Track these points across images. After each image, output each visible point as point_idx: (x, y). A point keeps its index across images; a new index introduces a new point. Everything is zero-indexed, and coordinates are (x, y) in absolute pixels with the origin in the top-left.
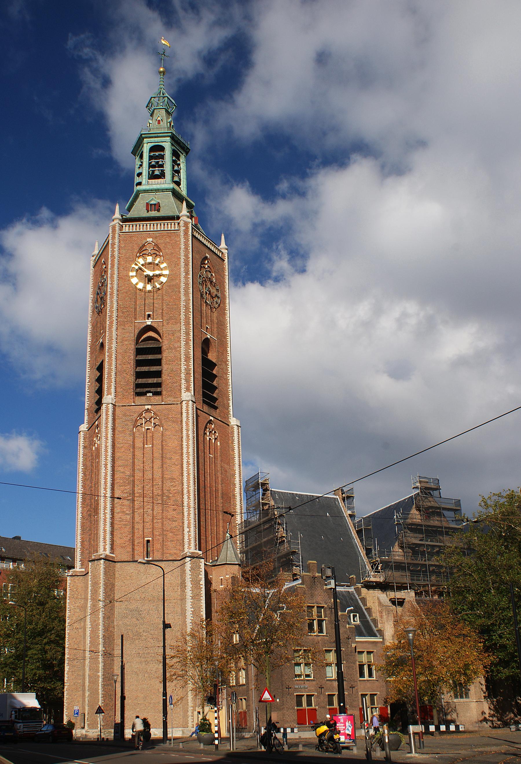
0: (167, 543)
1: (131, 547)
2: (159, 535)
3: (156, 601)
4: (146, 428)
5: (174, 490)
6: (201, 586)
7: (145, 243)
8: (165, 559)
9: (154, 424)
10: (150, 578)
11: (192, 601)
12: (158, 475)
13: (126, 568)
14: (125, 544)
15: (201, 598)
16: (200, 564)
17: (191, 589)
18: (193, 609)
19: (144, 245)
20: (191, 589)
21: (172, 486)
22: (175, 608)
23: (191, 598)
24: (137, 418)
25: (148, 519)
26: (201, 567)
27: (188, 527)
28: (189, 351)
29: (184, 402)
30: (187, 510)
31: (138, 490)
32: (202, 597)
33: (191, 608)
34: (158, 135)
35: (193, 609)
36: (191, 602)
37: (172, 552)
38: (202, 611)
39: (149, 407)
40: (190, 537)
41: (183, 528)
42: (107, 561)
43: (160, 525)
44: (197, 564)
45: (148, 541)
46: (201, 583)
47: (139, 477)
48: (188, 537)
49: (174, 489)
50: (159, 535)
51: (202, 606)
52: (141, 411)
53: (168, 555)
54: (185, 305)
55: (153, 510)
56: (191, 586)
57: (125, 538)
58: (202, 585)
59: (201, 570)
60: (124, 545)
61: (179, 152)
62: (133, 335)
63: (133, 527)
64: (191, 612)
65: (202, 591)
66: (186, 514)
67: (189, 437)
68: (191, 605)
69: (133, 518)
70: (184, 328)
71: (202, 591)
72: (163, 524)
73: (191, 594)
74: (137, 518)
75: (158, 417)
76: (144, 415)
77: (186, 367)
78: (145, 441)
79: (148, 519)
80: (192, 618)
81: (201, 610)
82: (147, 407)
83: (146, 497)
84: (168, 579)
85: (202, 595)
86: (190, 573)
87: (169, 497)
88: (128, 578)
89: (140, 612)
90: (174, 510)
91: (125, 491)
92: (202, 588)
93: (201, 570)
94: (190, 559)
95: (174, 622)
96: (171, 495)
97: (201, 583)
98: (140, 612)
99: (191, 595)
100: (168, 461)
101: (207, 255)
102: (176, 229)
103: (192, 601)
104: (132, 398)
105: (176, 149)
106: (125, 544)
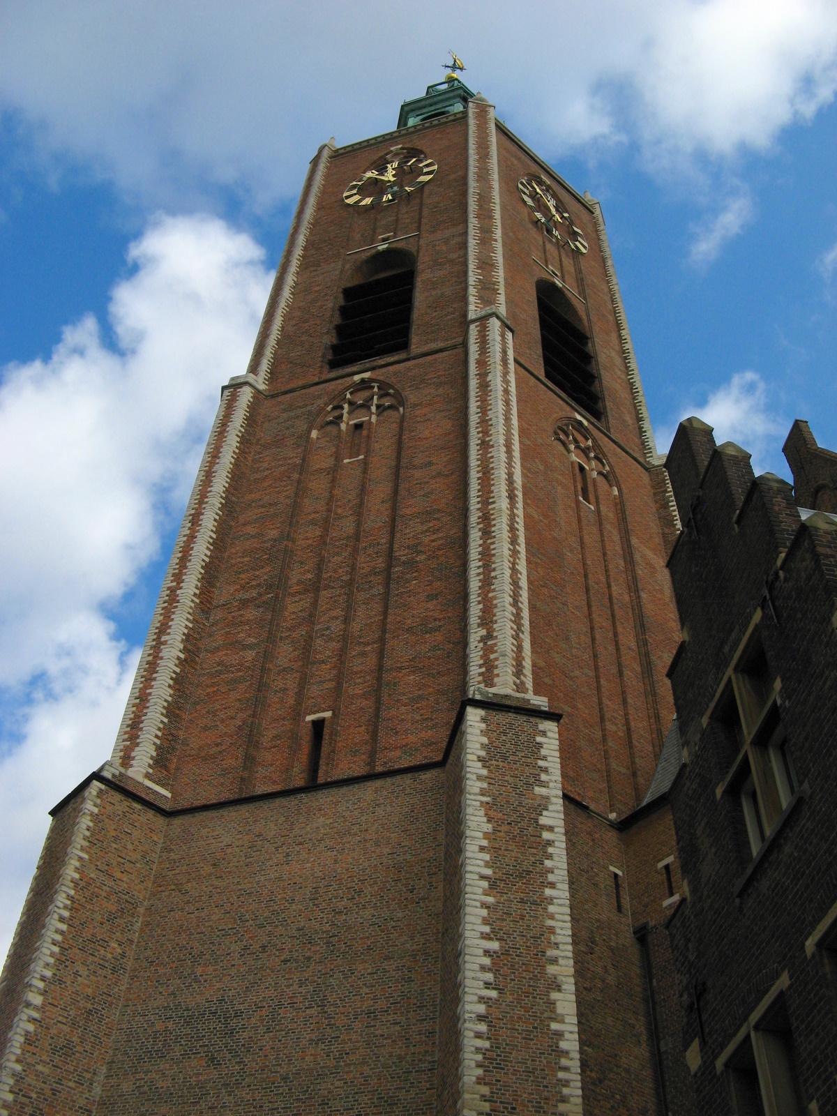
0: (393, 712)
1: (241, 753)
2: (364, 696)
3: (317, 957)
4: (352, 422)
5: (433, 541)
6: (546, 835)
7: (387, 154)
8: (379, 769)
9: (378, 407)
10: (304, 855)
11: (490, 900)
12: (376, 515)
13: (204, 832)
14: (217, 745)
15: (548, 892)
16: (539, 739)
17: (485, 843)
18: (495, 945)
20: (485, 843)
21: (426, 531)
22: (410, 980)
23: (485, 884)
25: (325, 649)
26: (543, 752)
27: (479, 625)
29: (472, 327)
30: (481, 570)
31: (299, 574)
32: (552, 885)
33: (485, 937)
34: (435, 99)
35: (495, 945)
36: (484, 905)
37: (412, 738)
38: (554, 961)
40: (492, 656)
41: (466, 625)
42: (117, 797)
43: (372, 660)
44: (523, 737)
45: (318, 725)
46: (543, 821)
47: (310, 542)
48: (485, 656)
49: (435, 536)
50: (364, 696)
51: (552, 930)
53: (398, 753)
54: (479, 194)
55: (347, 620)
56: (488, 827)
57: (221, 727)
58: (551, 829)
59: (541, 763)
60: (214, 750)
63: (262, 687)
64: (487, 961)
65: (550, 857)
66: (474, 584)
68: (485, 921)
69: (267, 656)
71: (550, 857)
72: (381, 654)
73: (487, 865)
74: (285, 653)
75: (391, 391)
76: (348, 396)
79: (325, 649)
80: (493, 994)
81: (551, 953)
83: (327, 587)
84: (386, 850)
85: (551, 878)
86: (485, 772)
87: (411, 564)
88: (208, 869)
89: (233, 1023)
90: (431, 597)
91: (254, 583)
92: (550, 843)
93: (541, 763)
94: (481, 712)
95: (400, 1058)
96: (422, 557)
97: (543, 821)
98: (233, 1023)
99: (489, 872)
100: (417, 474)
103: (490, 900)
106: (217, 745)
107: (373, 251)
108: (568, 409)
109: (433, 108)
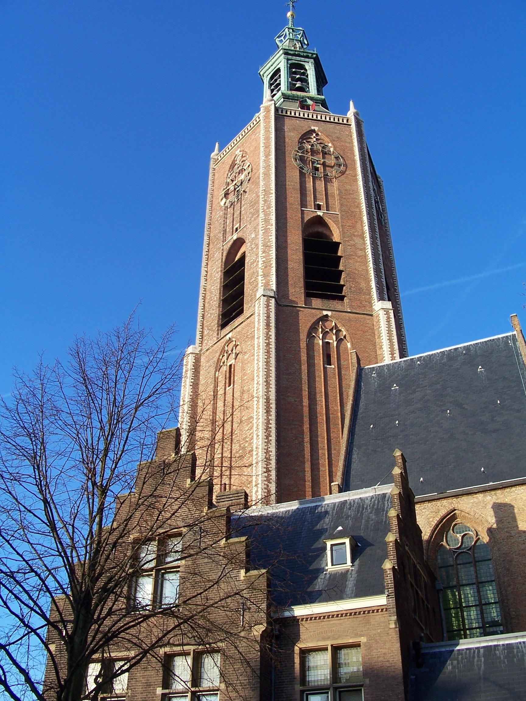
4: (228, 364)
7: (235, 157)
19: (234, 161)
21: (248, 430)
24: (219, 356)
28: (270, 237)
39: (230, 335)
52: (223, 344)
54: (264, 190)
61: (302, 63)
62: (220, 261)
67: (259, 346)
70: (263, 216)
77: (264, 259)
78: (227, 382)
82: (227, 337)
101: (313, 128)
102: (258, 120)
104: (216, 334)
105: (296, 62)
107: (232, 241)
108: (318, 312)
109: (273, 67)
